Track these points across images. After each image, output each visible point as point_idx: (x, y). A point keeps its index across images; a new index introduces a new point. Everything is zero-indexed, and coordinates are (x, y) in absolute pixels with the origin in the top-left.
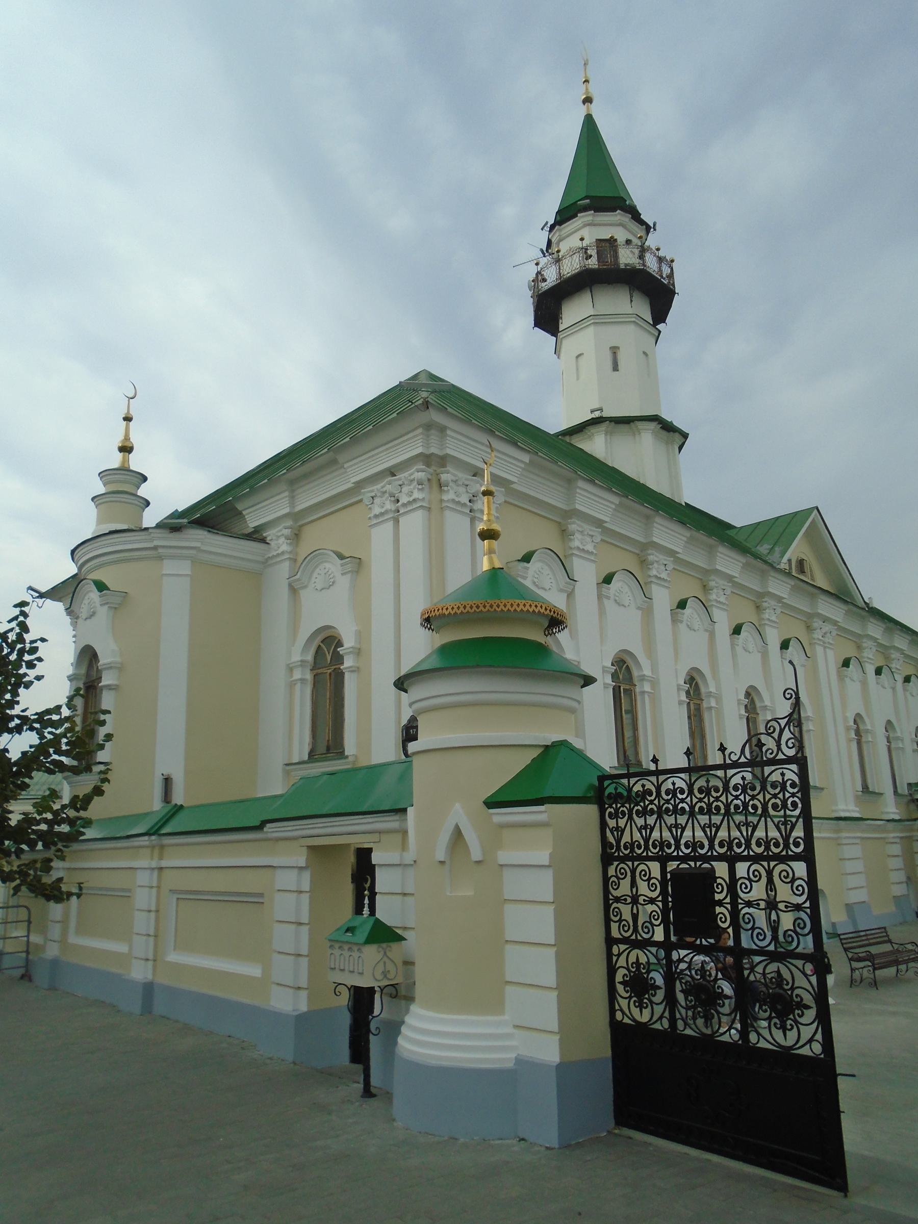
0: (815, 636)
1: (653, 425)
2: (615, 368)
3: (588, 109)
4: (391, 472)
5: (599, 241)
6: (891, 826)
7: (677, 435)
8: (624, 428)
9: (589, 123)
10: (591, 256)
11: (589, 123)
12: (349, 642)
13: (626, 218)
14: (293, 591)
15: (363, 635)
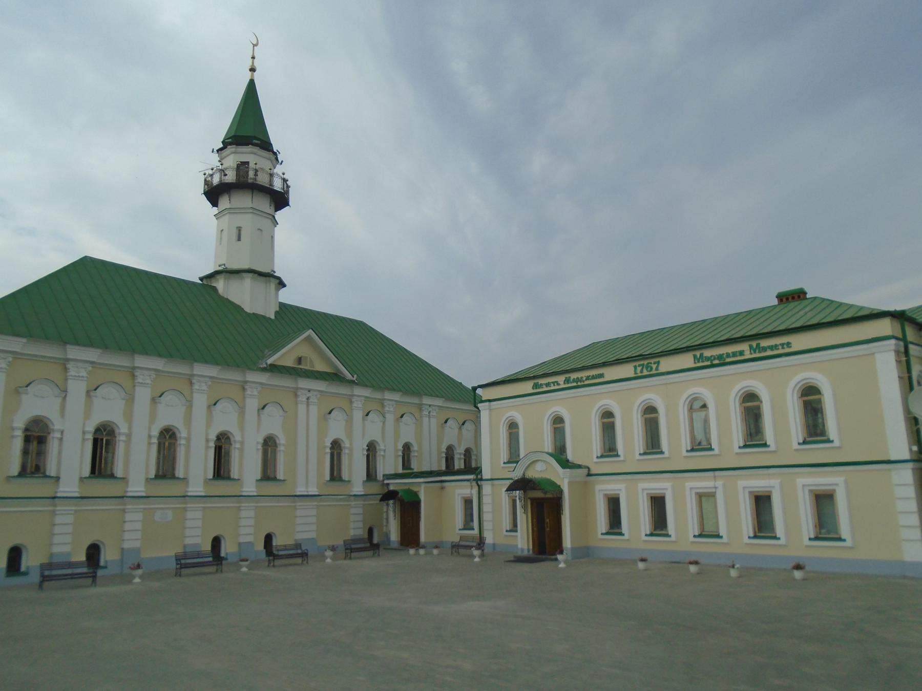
0: (300, 399)
1: (250, 275)
2: (239, 239)
3: (252, 75)
6: (352, 498)
7: (272, 279)
9: (251, 86)
10: (225, 175)
11: (251, 86)
13: (256, 150)
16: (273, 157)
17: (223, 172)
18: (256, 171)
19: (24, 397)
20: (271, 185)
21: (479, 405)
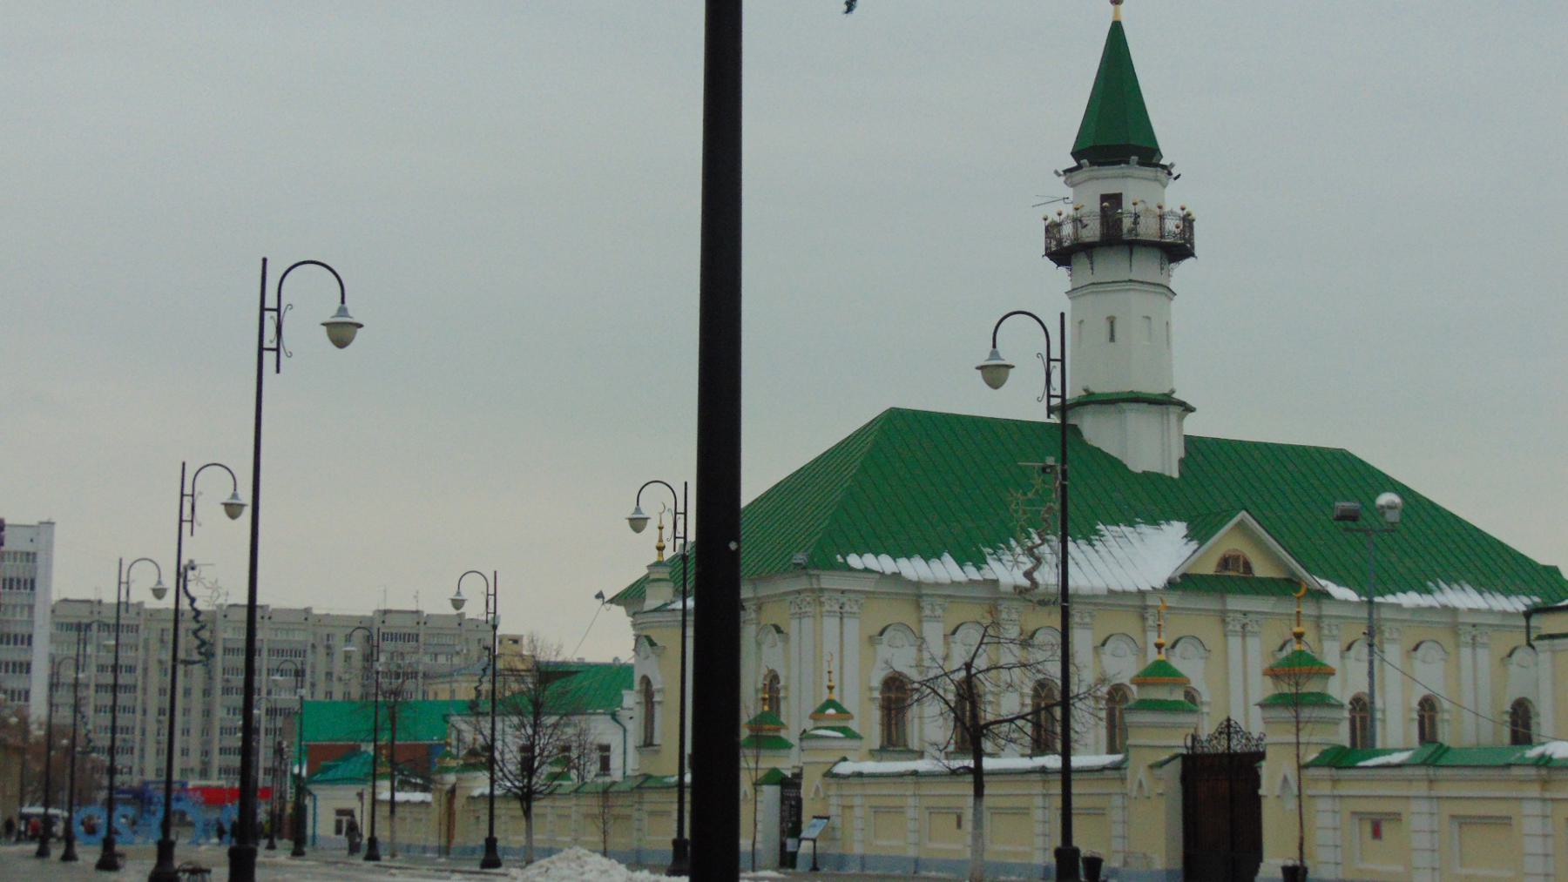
1: (1135, 406)
3: (1116, 13)
4: (799, 592)
5: (1104, 198)
7: (1172, 408)
8: (1111, 408)
12: (782, 683)
14: (759, 644)
15: (788, 678)
16: (1162, 175)
17: (1077, 221)
18: (1137, 216)
19: (878, 647)
20: (1162, 236)
21: (1535, 644)
